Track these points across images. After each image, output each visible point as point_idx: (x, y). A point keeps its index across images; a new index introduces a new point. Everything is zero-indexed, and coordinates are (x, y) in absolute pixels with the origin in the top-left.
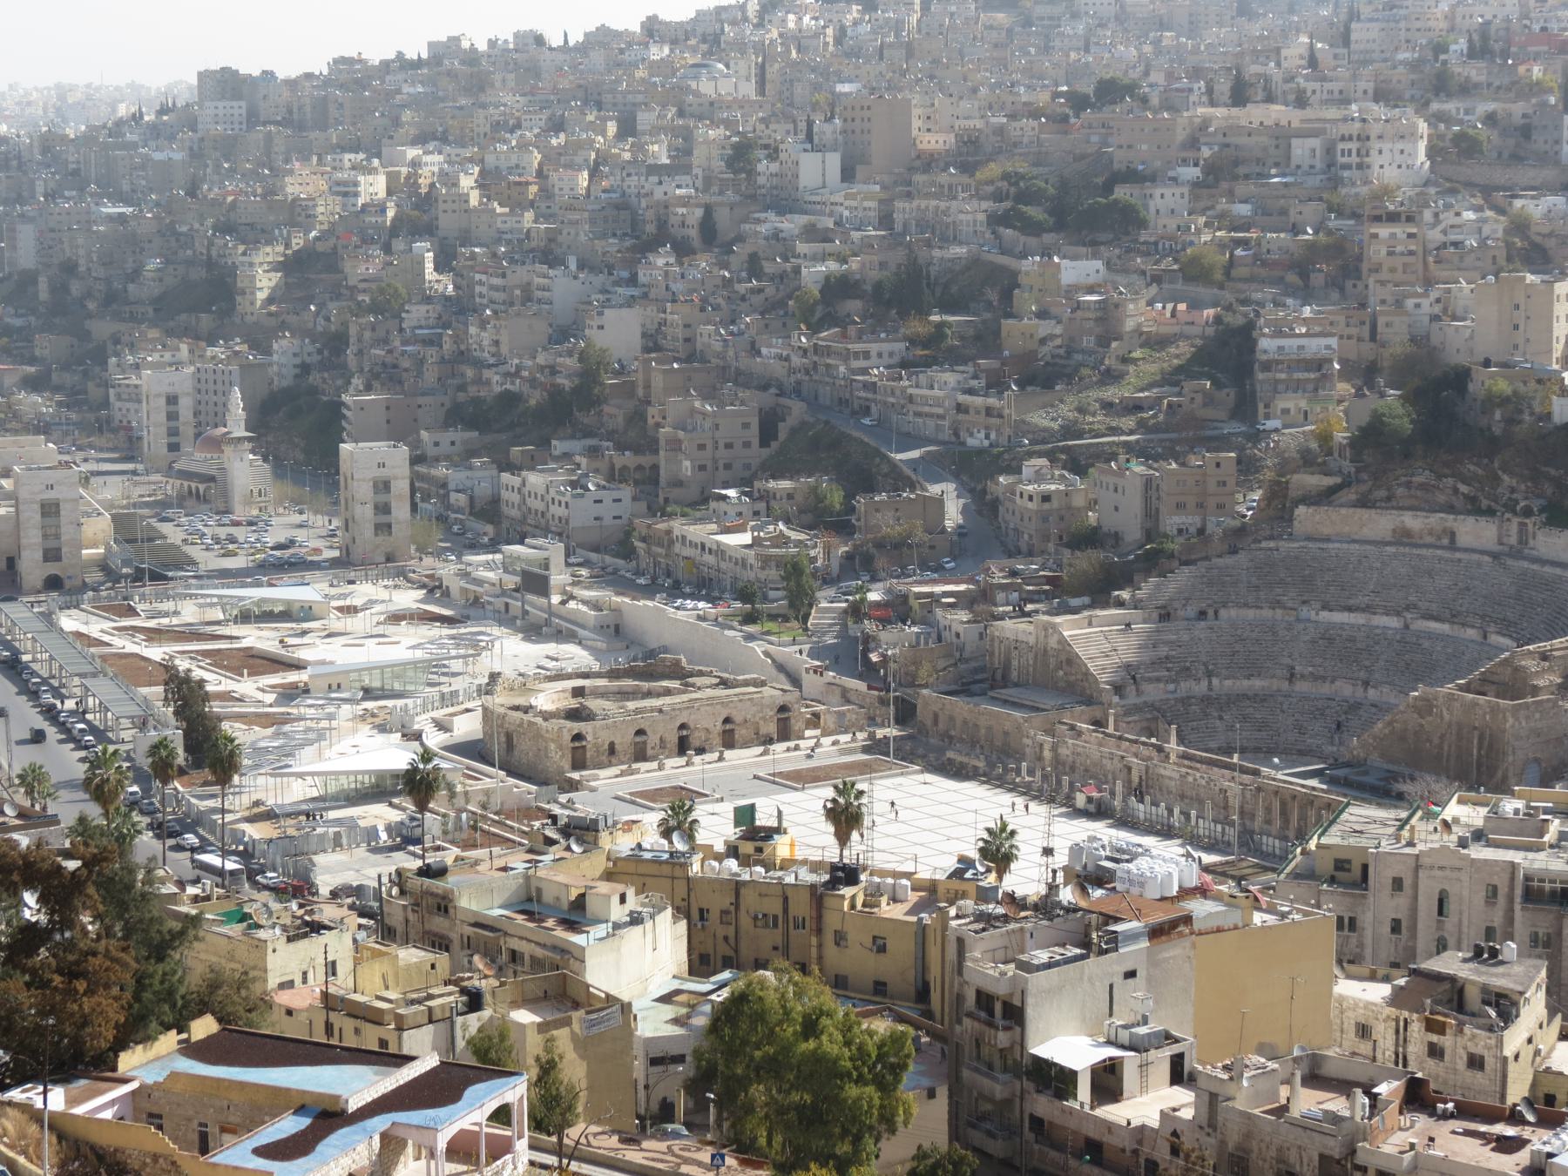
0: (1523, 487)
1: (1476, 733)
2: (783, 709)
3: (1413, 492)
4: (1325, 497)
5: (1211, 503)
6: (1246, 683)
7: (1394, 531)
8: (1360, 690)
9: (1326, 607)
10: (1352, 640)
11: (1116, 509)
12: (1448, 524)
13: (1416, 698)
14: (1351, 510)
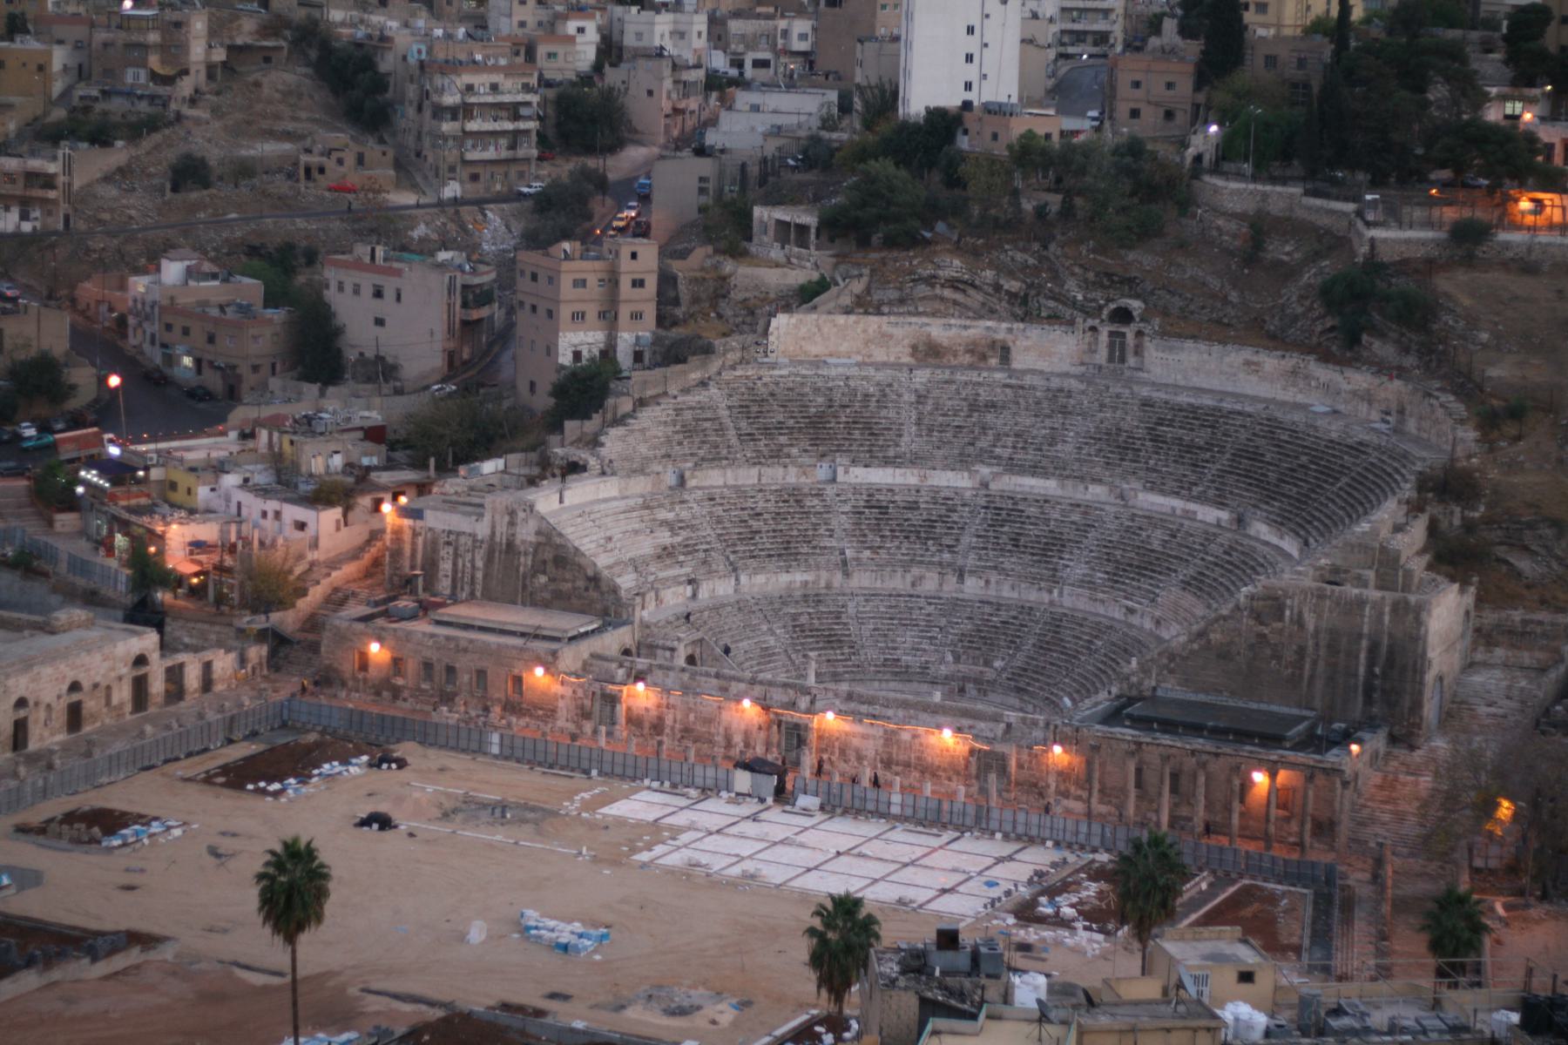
1: (1364, 643)
2: (141, 660)
3: (938, 291)
4: (806, 296)
5: (624, 312)
6: (784, 578)
8: (952, 579)
9: (854, 462)
10: (913, 506)
11: (380, 322)
12: (1000, 336)
13: (1252, 597)
14: (853, 318)
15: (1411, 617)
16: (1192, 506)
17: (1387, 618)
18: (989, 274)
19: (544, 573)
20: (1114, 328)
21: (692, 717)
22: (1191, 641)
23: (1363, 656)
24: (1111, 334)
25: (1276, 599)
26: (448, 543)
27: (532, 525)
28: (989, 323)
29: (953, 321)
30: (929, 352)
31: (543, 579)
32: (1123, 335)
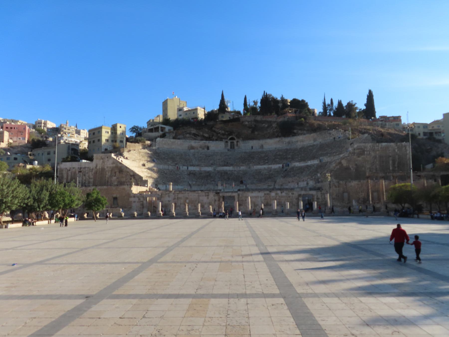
0: (227, 133)
1: (391, 158)
7: (188, 147)
12: (207, 144)
14: (174, 140)
15: (404, 148)
16: (270, 166)
17: (396, 151)
18: (201, 133)
19: (115, 176)
20: (231, 141)
21: (187, 201)
22: (336, 166)
23: (391, 162)
24: (231, 143)
25: (362, 149)
26: (80, 172)
27: (111, 161)
28: (204, 141)
29: (197, 141)
30: (192, 148)
31: (114, 178)
32: (233, 142)
